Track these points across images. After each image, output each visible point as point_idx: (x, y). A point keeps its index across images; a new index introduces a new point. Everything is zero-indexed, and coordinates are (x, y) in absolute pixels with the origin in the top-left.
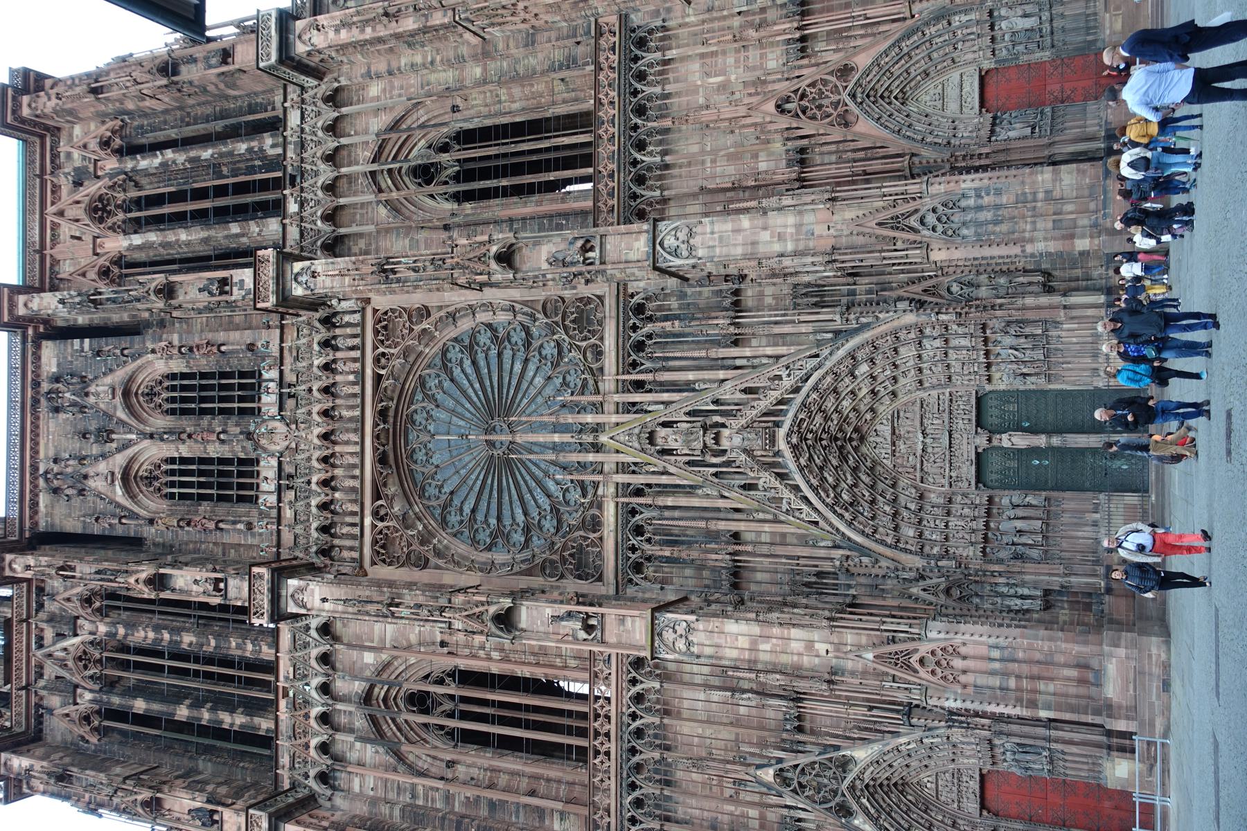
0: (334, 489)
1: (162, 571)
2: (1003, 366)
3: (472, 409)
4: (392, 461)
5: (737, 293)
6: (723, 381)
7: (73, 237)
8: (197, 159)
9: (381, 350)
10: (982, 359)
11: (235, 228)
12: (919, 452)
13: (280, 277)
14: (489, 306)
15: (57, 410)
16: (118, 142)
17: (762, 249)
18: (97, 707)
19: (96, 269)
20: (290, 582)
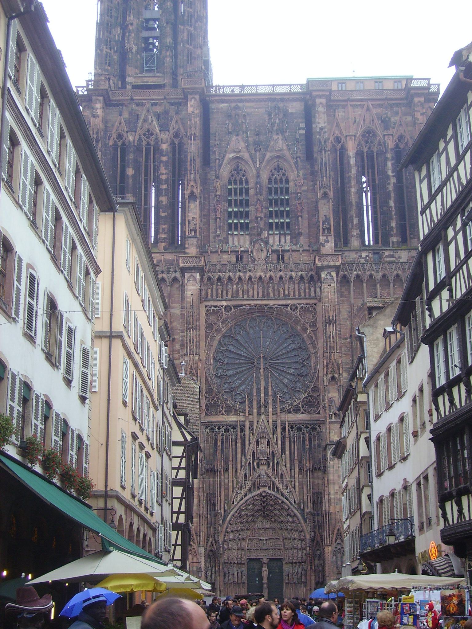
0: (238, 283)
1: (198, 201)
2: (291, 568)
3: (274, 349)
4: (250, 311)
5: (319, 469)
6: (286, 466)
7: (355, 121)
8: (388, 197)
9: (299, 307)
10: (294, 561)
11: (356, 221)
12: (260, 538)
13: (329, 267)
14: (316, 363)
15: (270, 115)
16: (402, 146)
17: (331, 486)
18: (126, 142)
19: (340, 136)
20: (198, 274)
